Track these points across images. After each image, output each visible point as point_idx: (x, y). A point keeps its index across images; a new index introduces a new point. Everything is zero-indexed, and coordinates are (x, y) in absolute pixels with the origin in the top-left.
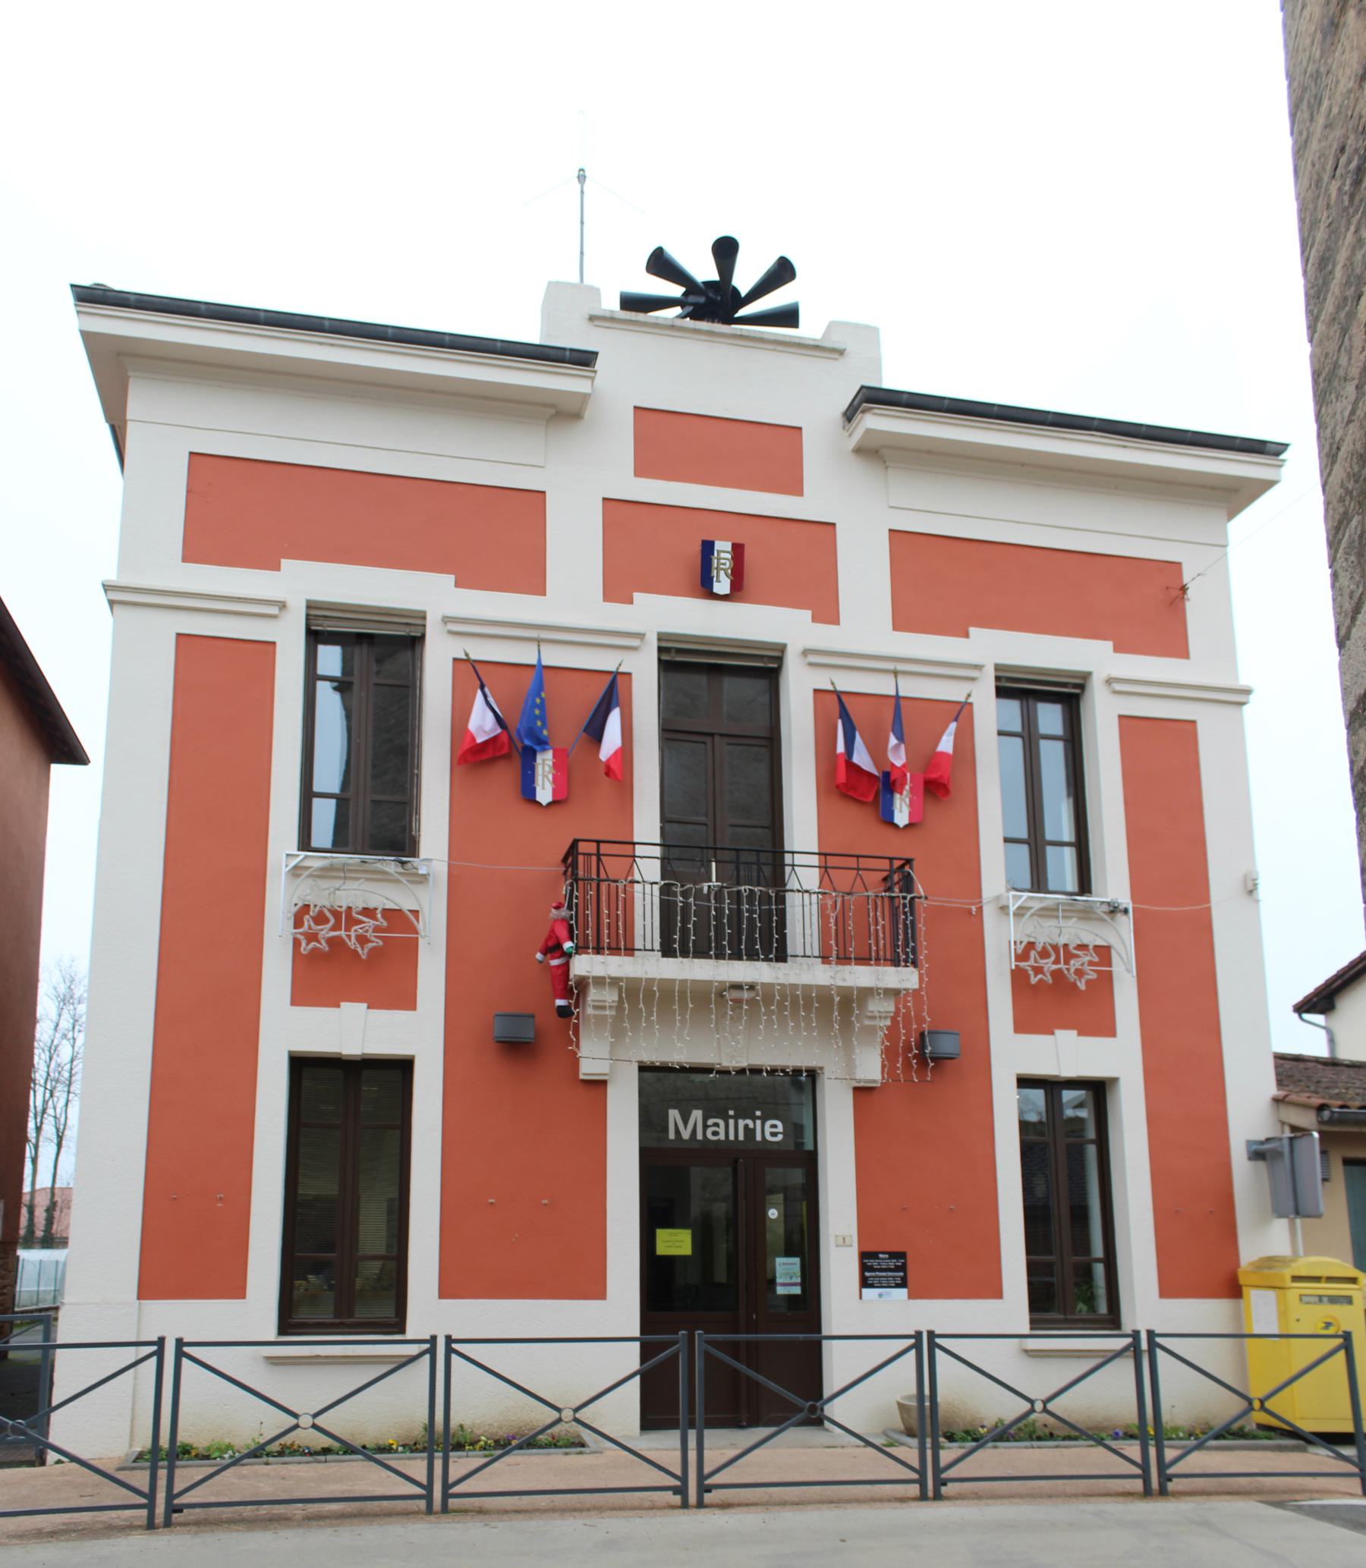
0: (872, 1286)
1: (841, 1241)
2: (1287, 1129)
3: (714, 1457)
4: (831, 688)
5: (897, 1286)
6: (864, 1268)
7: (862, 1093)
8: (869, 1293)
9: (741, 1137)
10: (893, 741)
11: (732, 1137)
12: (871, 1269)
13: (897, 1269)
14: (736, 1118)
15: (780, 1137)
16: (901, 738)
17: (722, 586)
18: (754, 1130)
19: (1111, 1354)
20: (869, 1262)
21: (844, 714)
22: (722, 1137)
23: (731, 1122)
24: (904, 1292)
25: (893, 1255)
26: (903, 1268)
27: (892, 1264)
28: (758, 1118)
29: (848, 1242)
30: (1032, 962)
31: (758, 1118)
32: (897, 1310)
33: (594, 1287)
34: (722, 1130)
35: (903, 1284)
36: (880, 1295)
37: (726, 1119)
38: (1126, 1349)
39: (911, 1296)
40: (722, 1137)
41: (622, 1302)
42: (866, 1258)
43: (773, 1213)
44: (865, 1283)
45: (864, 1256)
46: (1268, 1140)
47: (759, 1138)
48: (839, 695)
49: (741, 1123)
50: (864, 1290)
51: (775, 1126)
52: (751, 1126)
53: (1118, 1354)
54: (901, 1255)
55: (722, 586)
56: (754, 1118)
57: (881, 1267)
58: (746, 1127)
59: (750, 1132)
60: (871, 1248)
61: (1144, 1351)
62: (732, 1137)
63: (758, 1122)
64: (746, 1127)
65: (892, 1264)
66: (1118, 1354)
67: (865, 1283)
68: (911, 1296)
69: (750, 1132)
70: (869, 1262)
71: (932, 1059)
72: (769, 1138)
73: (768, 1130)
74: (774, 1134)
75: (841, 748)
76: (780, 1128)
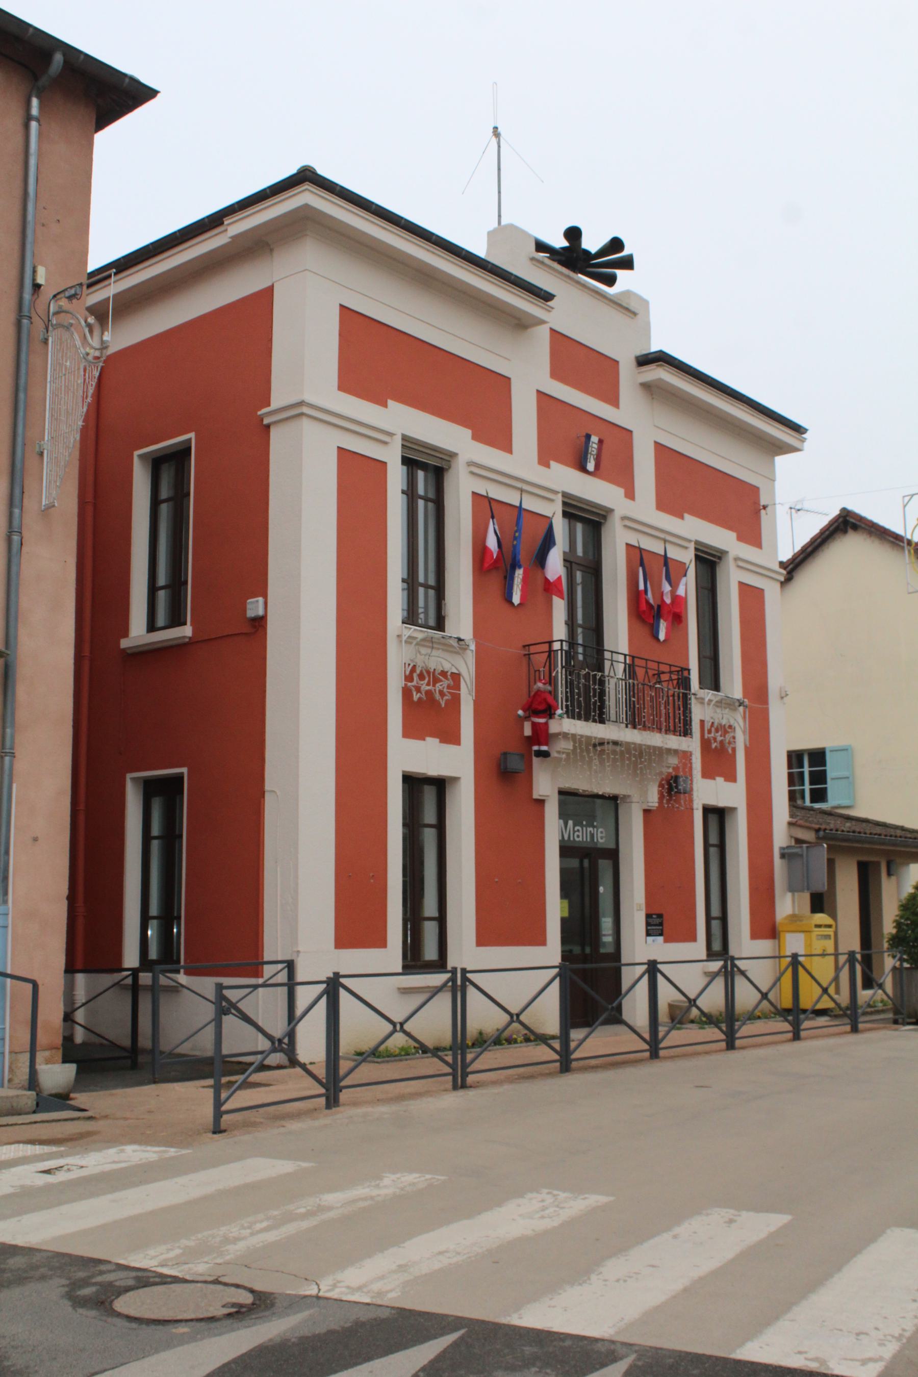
4: (637, 545)
6: (648, 924)
8: (650, 939)
14: (587, 826)
17: (591, 466)
19: (436, 990)
20: (650, 920)
21: (642, 564)
24: (661, 939)
26: (661, 924)
35: (661, 935)
37: (582, 826)
38: (445, 985)
39: (666, 941)
40: (580, 839)
41: (551, 951)
43: (601, 889)
44: (648, 934)
45: (648, 916)
48: (641, 550)
53: (436, 991)
54: (660, 916)
55: (591, 466)
56: (594, 827)
61: (459, 986)
66: (436, 991)
67: (648, 934)
68: (666, 941)
70: (650, 920)
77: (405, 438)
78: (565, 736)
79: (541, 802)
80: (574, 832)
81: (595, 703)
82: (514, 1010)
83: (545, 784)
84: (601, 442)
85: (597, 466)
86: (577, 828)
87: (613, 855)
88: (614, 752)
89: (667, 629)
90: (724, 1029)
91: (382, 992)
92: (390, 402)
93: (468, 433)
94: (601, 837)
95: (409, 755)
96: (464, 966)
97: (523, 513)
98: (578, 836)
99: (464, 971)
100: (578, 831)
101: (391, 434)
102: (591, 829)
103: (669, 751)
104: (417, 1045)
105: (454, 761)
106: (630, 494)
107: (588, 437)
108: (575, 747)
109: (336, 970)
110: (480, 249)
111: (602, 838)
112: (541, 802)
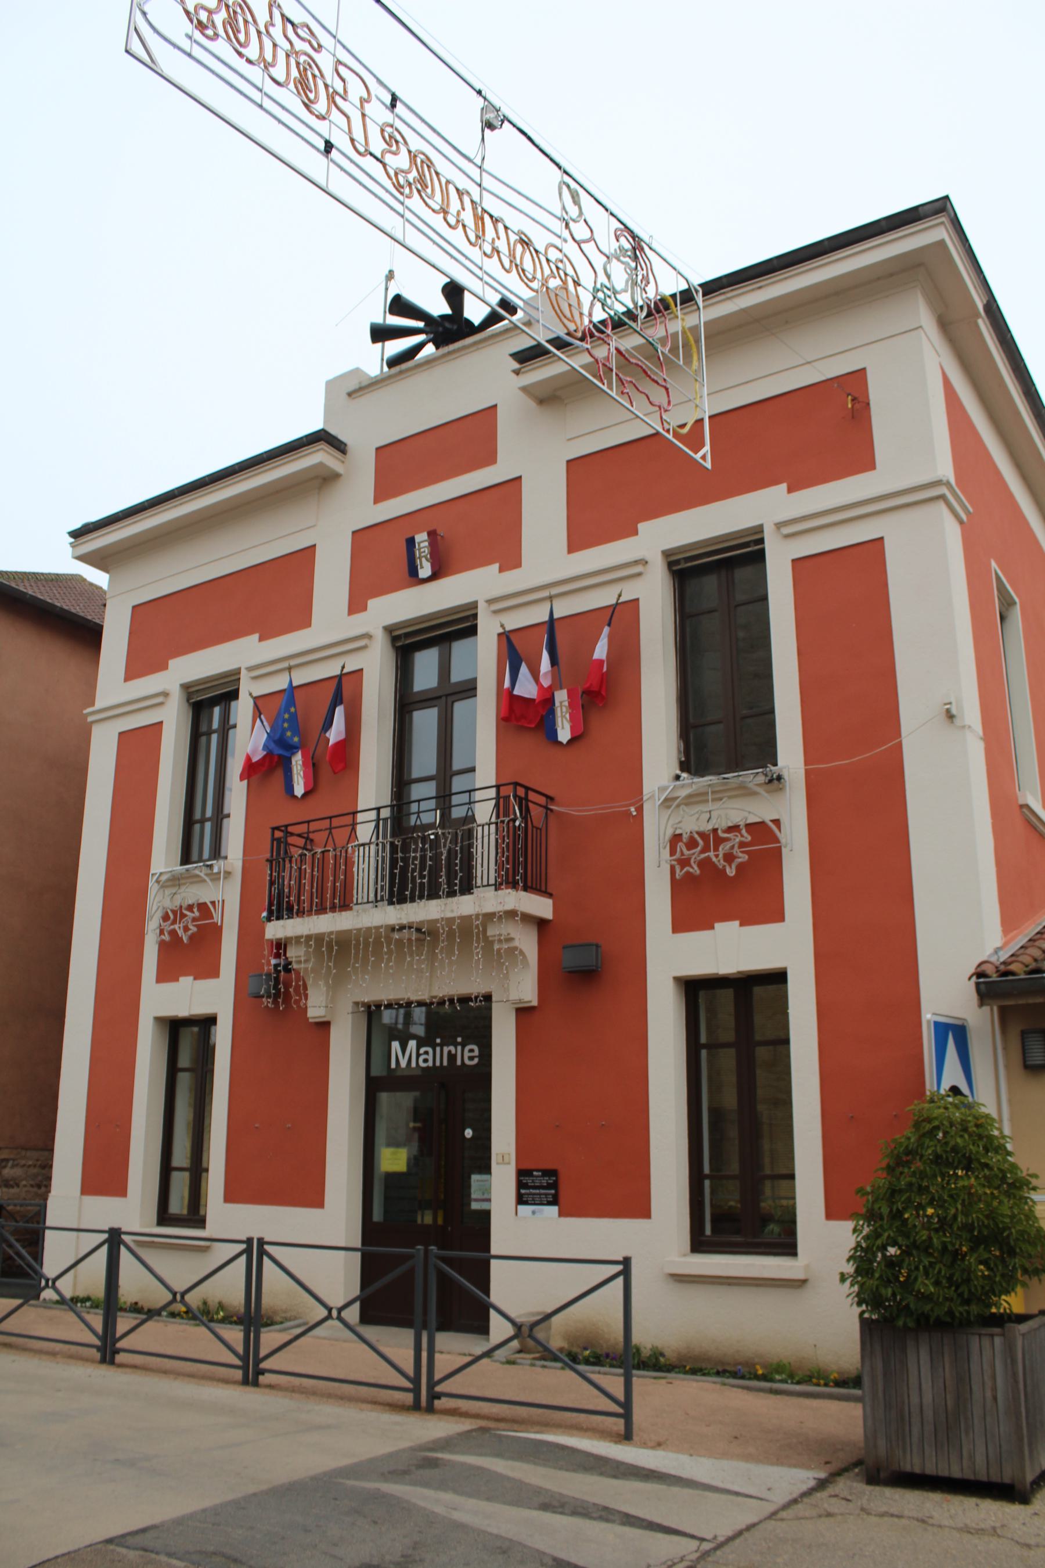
0: (526, 1203)
1: (501, 1160)
3: (444, 1363)
5: (549, 1203)
6: (520, 1185)
7: (523, 1012)
8: (522, 1208)
9: (445, 1063)
11: (438, 1064)
12: (526, 1186)
13: (549, 1186)
14: (442, 1045)
15: (476, 1060)
17: (425, 571)
18: (455, 1055)
20: (528, 1180)
22: (430, 1064)
23: (438, 1049)
24: (554, 1210)
25: (547, 1173)
26: (554, 1186)
27: (545, 1181)
28: (459, 1044)
29: (506, 1160)
31: (459, 1044)
34: (430, 1058)
35: (554, 1202)
36: (534, 1213)
37: (434, 1046)
39: (561, 1214)
40: (430, 1064)
42: (523, 1174)
44: (521, 1200)
47: (459, 1062)
49: (446, 1049)
50: (520, 1207)
51: (472, 1051)
52: (453, 1052)
57: (537, 1185)
58: (450, 1052)
59: (452, 1057)
60: (527, 1165)
62: (438, 1064)
63: (459, 1048)
64: (450, 1052)
65: (545, 1181)
67: (521, 1200)
68: (561, 1214)
69: (452, 1057)
70: (528, 1180)
71: (589, 970)
72: (467, 1062)
73: (467, 1054)
74: (471, 1058)
75: (507, 684)
76: (476, 1053)
80: (418, 1055)
81: (422, 877)
84: (432, 534)
86: (422, 1051)
88: (399, 942)
94: (468, 1055)
95: (163, 998)
97: (513, 637)
100: (426, 1053)
102: (452, 1048)
105: (213, 996)
107: (411, 542)
111: (471, 1058)
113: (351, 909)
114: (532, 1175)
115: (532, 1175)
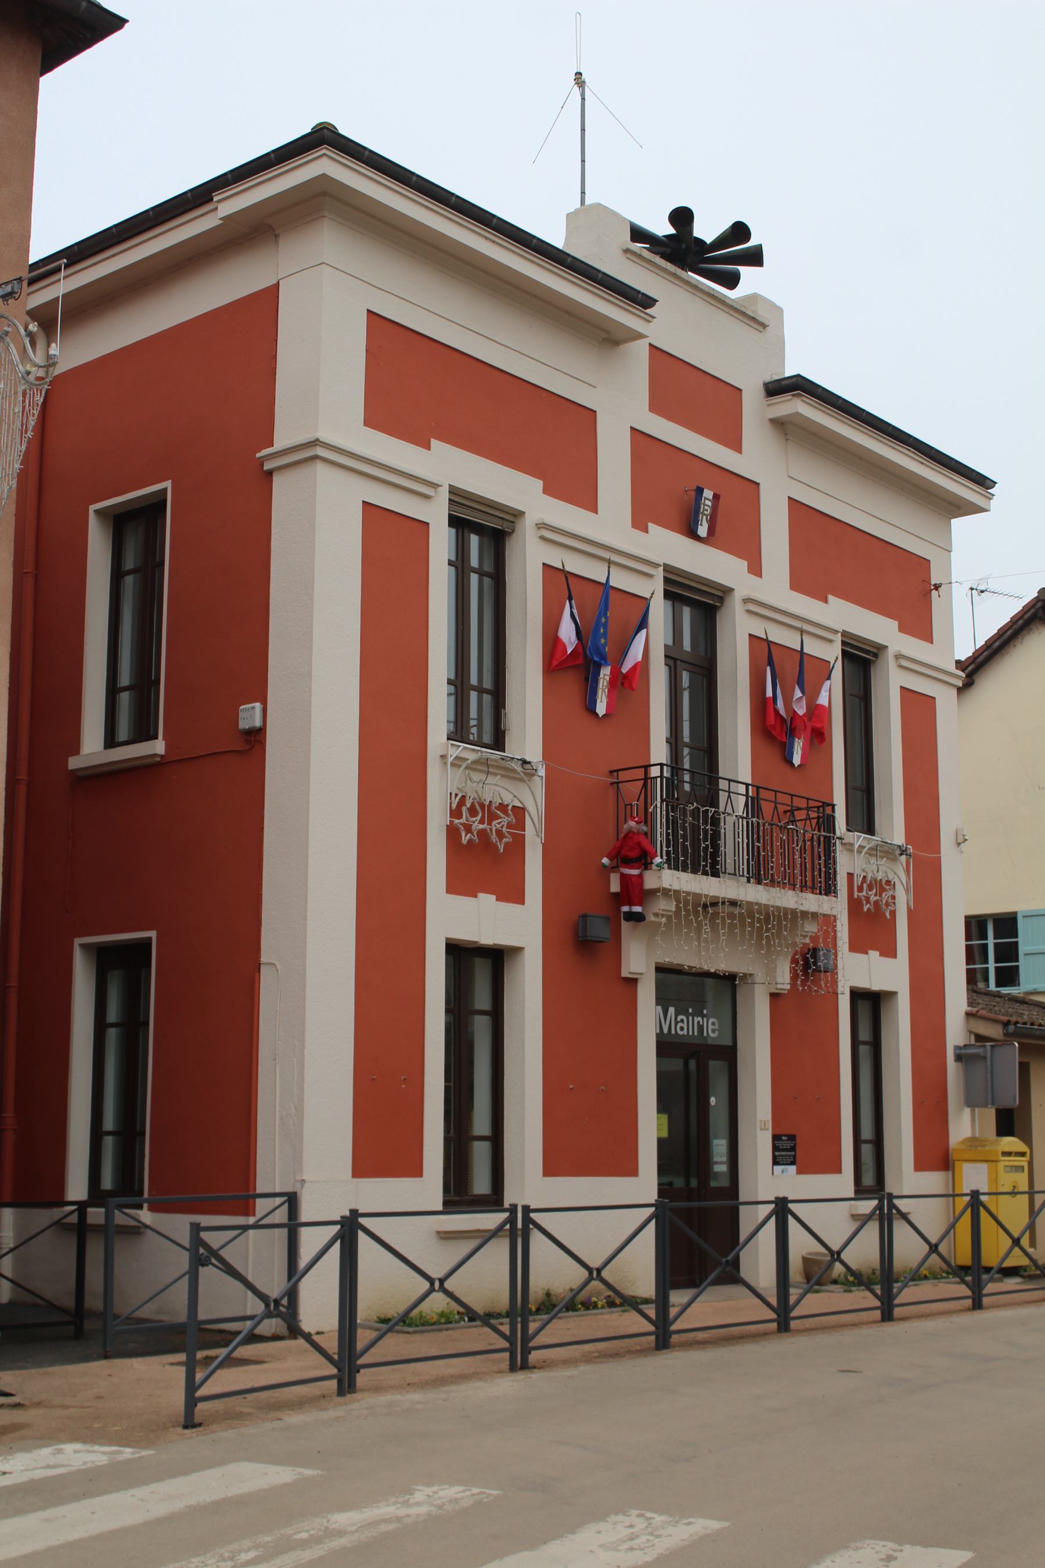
2: (973, 1038)
6: (775, 1148)
7: (774, 996)
8: (778, 1169)
10: (798, 693)
14: (693, 1015)
16: (803, 692)
17: (703, 531)
19: (487, 1235)
20: (779, 1143)
21: (770, 662)
24: (794, 1167)
26: (793, 1149)
30: (864, 893)
32: (789, 1182)
33: (631, 1170)
35: (793, 1163)
37: (687, 1015)
38: (500, 1228)
39: (799, 1172)
41: (645, 1185)
43: (713, 1100)
45: (776, 1138)
46: (965, 1046)
53: (488, 1237)
54: (792, 1138)
55: (703, 531)
56: (703, 1016)
60: (778, 1132)
61: (520, 1229)
66: (488, 1237)
67: (776, 1162)
68: (799, 1172)
70: (779, 1143)
75: (769, 693)
77: (453, 491)
78: (666, 892)
79: (632, 982)
80: (676, 1023)
81: (706, 848)
82: (594, 1264)
83: (638, 958)
84: (716, 497)
85: (711, 531)
86: (679, 1018)
87: (729, 1054)
88: (731, 916)
89: (803, 749)
90: (879, 1292)
91: (414, 1237)
92: (434, 442)
93: (539, 484)
94: (712, 1029)
95: (456, 916)
96: (526, 1203)
98: (682, 1029)
99: (527, 1209)
100: (682, 1021)
101: (435, 486)
102: (700, 1019)
103: (805, 914)
104: (462, 1310)
105: (516, 923)
106: (756, 569)
107: (700, 491)
108: (677, 906)
109: (353, 1207)
110: (557, 238)
111: (713, 1031)
112: (632, 982)
113: (719, 876)
114: (781, 1140)
115: (781, 1140)
